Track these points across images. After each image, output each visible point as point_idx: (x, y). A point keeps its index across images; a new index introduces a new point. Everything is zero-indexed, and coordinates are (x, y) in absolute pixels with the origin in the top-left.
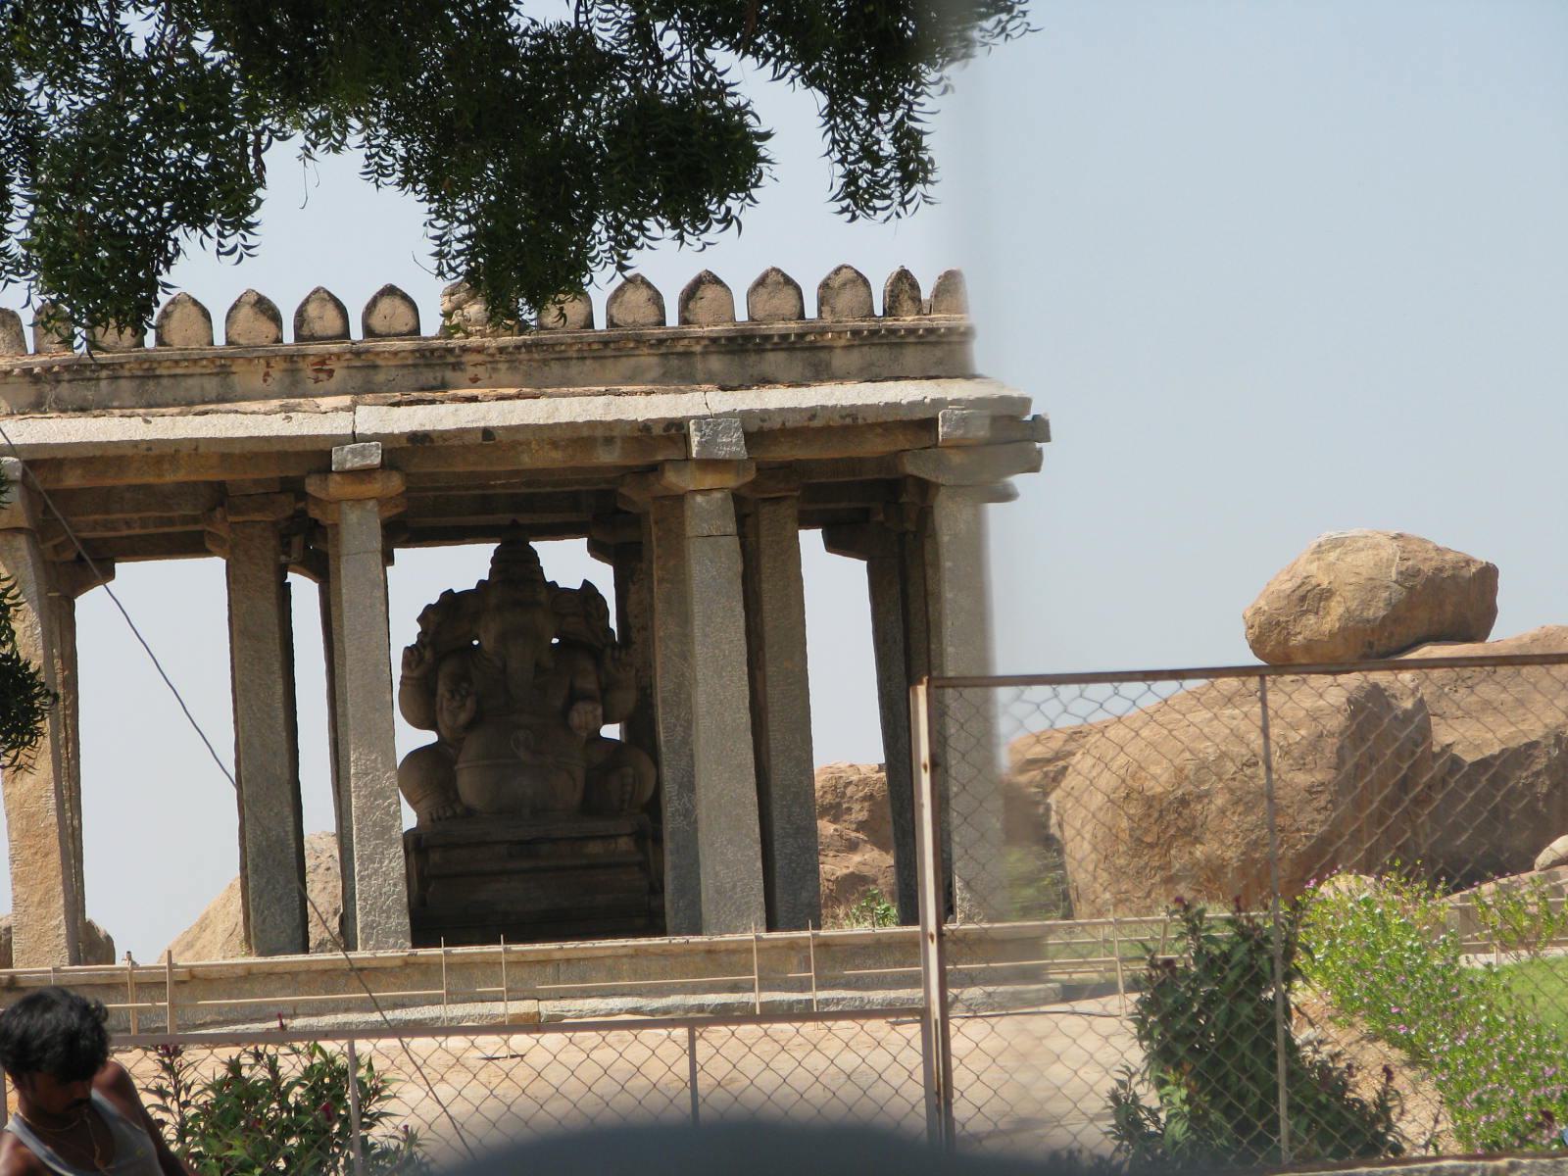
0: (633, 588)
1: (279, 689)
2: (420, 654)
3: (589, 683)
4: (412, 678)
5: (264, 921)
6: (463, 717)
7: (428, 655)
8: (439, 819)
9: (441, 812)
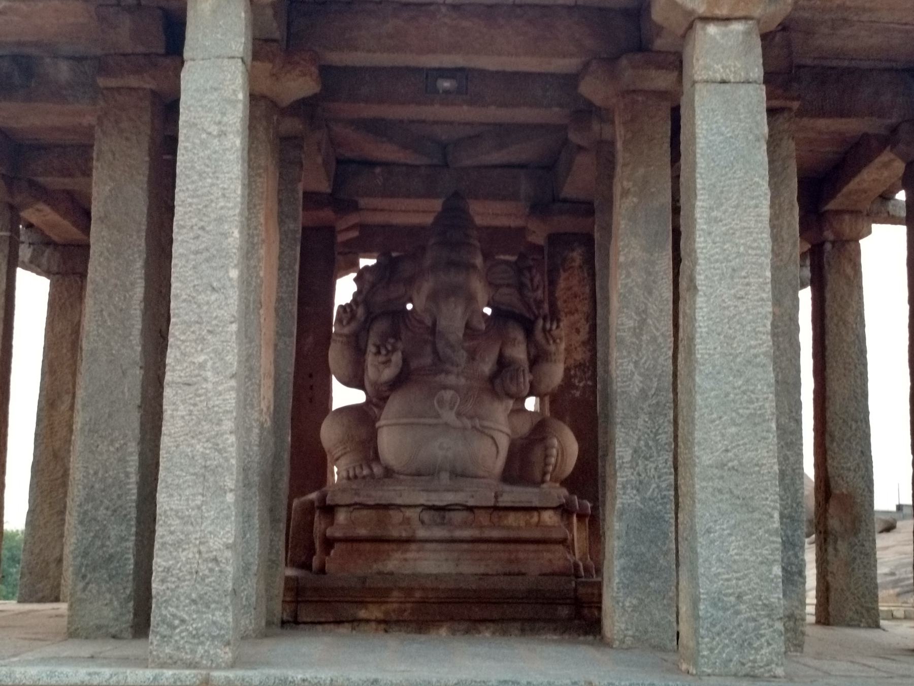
0: (563, 275)
1: (139, 291)
2: (352, 310)
3: (519, 353)
4: (341, 335)
5: (84, 589)
6: (388, 373)
7: (360, 311)
8: (356, 477)
9: (358, 471)
